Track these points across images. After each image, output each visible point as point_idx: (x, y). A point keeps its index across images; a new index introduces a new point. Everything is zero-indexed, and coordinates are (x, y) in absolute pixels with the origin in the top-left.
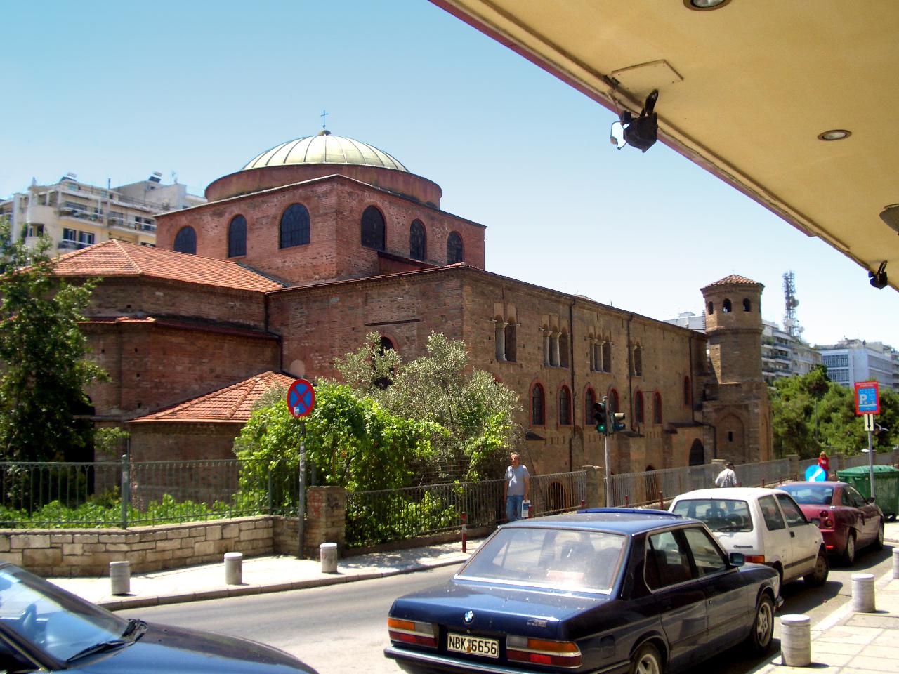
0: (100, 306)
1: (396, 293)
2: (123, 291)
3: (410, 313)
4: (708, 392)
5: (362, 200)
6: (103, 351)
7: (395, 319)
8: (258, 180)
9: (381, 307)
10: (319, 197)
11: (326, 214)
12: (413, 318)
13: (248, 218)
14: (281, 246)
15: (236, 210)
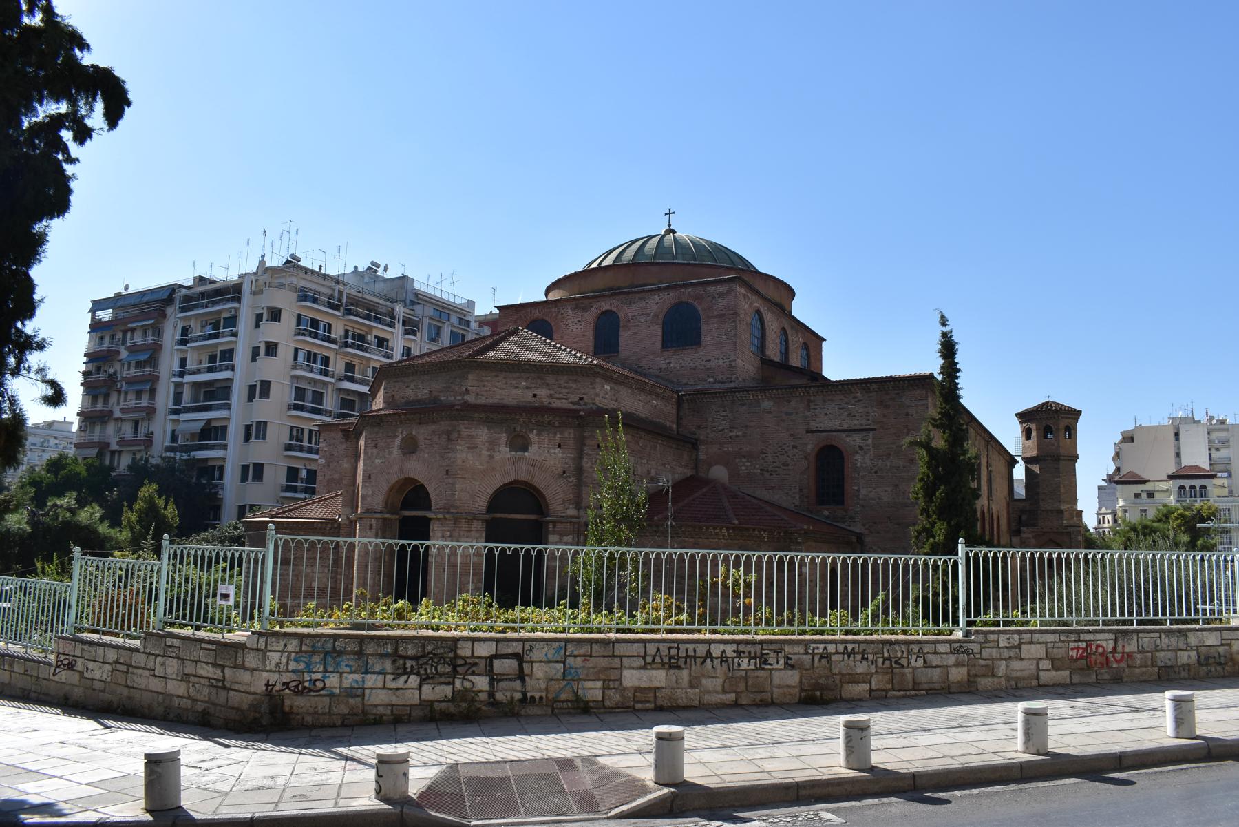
0: (551, 396)
2: (575, 381)
3: (864, 422)
4: (1024, 518)
5: (751, 304)
6: (559, 446)
7: (845, 426)
11: (723, 315)
13: (621, 315)
14: (663, 347)
15: (606, 306)
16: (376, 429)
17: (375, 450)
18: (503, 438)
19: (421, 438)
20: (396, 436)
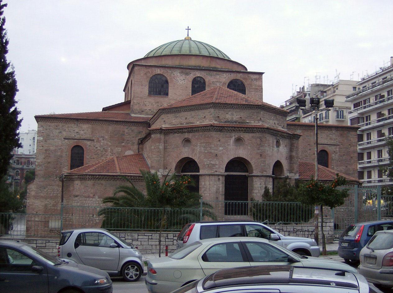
1: (329, 133)
3: (335, 142)
7: (329, 143)
8: (209, 62)
9: (322, 138)
10: (252, 80)
11: (257, 89)
12: (337, 144)
15: (198, 74)
16: (219, 133)
17: (218, 143)
18: (275, 141)
19: (246, 139)
20: (231, 137)
